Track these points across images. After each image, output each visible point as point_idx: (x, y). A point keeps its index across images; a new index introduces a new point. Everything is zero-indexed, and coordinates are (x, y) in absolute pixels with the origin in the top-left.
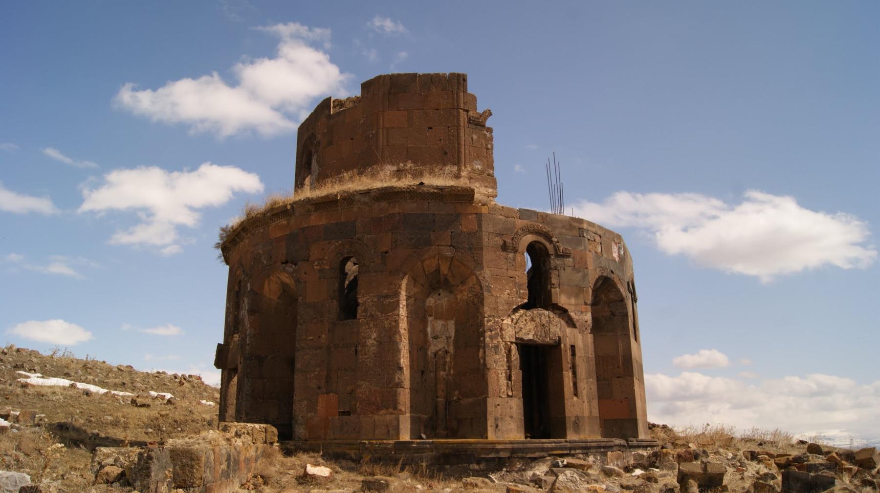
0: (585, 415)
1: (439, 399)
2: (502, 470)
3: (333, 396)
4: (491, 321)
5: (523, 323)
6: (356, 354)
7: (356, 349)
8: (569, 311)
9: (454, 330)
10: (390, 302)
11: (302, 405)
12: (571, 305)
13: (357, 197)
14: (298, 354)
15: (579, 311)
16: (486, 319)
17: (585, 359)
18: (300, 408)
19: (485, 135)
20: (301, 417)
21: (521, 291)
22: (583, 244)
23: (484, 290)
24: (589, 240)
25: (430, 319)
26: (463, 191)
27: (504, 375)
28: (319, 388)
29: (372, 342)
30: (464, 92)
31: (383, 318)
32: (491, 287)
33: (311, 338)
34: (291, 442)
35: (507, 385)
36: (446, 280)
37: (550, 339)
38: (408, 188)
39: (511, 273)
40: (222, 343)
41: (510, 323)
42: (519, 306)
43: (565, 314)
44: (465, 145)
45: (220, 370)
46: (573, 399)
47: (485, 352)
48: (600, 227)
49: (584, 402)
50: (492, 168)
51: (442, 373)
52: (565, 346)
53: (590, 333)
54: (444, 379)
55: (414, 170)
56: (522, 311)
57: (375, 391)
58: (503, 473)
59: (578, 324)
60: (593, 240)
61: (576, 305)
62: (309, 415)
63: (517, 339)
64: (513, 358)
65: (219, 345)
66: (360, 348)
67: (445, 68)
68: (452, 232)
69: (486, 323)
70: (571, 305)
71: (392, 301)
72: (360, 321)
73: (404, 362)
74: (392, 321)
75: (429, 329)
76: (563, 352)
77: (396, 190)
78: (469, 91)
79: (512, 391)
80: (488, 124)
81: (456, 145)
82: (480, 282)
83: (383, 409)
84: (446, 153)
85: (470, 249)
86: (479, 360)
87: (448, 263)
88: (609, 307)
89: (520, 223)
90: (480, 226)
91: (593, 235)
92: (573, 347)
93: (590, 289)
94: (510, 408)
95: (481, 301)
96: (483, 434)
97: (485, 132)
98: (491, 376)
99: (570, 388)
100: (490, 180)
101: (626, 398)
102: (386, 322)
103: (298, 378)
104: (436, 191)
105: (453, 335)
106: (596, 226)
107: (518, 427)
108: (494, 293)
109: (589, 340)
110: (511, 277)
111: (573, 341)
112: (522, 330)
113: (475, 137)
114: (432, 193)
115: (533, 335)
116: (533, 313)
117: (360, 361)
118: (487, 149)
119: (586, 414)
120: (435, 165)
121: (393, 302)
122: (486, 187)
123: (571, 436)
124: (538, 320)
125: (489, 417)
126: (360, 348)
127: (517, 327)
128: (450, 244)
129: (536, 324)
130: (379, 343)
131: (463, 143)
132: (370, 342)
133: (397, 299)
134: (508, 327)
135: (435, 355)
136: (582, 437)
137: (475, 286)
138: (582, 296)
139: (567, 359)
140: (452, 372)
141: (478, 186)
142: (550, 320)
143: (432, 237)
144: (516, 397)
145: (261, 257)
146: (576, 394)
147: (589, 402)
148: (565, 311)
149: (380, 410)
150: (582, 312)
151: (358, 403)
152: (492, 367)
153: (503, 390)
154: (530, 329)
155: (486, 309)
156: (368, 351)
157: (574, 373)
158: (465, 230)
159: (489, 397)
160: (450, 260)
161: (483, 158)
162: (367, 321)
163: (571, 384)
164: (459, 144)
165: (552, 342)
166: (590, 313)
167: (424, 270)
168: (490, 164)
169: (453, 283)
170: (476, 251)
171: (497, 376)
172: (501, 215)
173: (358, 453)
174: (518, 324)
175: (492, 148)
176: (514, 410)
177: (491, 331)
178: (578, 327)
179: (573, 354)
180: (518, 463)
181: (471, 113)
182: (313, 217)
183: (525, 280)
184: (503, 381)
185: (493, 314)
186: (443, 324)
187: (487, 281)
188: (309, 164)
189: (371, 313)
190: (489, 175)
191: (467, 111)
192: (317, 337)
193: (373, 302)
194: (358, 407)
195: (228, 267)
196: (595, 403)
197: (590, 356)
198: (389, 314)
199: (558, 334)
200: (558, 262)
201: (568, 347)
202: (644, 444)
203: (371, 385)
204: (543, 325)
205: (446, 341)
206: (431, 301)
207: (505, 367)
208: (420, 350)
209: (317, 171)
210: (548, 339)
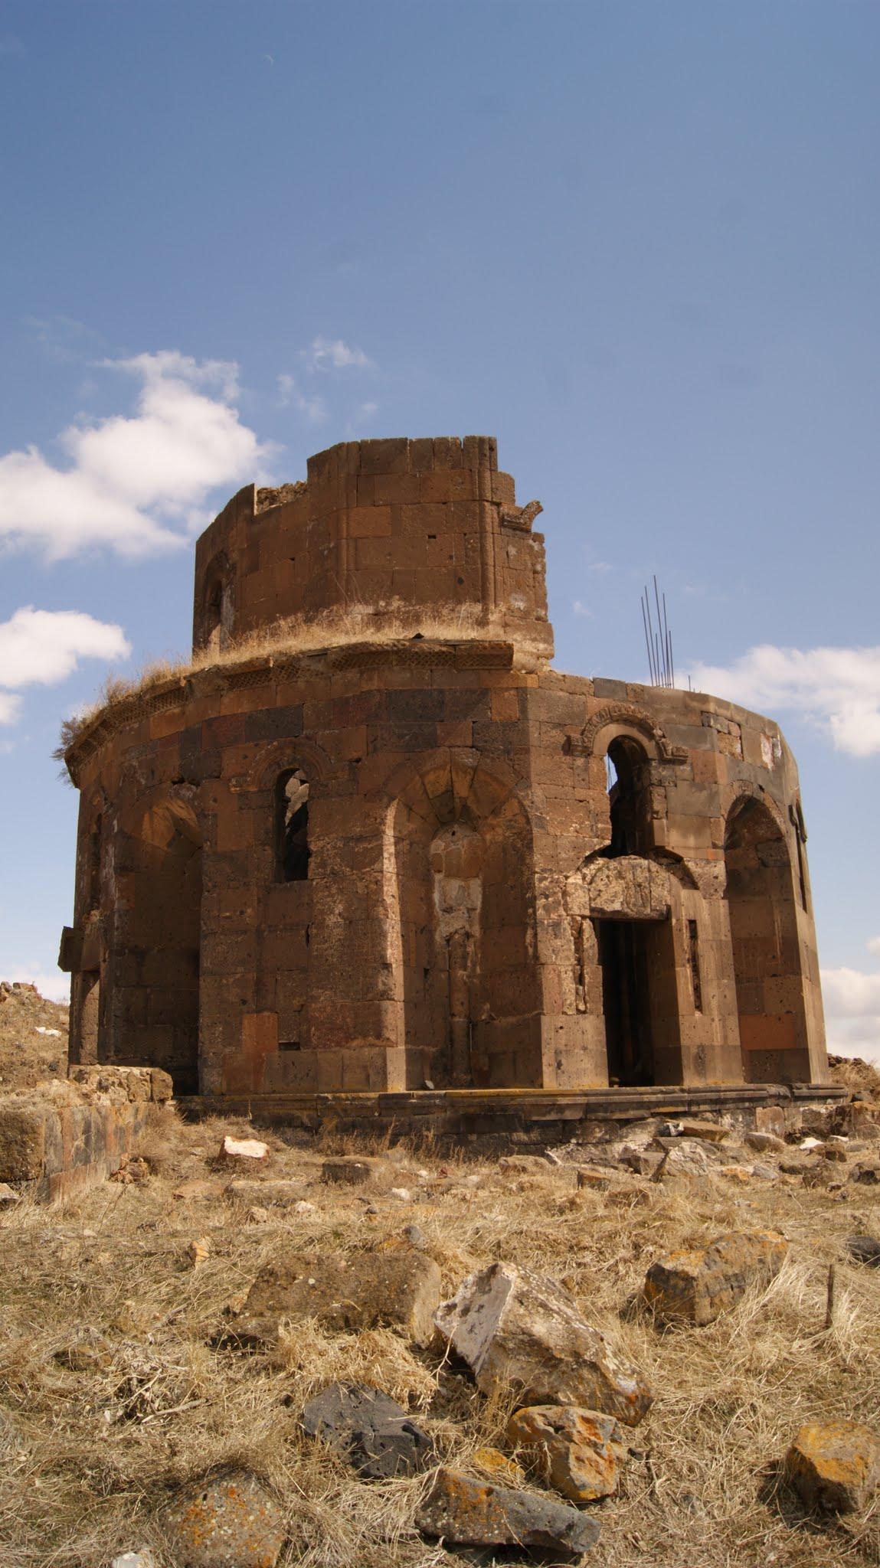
0: (715, 1044)
1: (456, 1019)
2: (570, 1142)
3: (269, 1017)
4: (545, 879)
5: (603, 883)
6: (308, 941)
7: (307, 931)
9: (480, 896)
10: (366, 849)
11: (214, 1034)
12: (689, 848)
13: (303, 663)
14: (206, 942)
15: (701, 859)
16: (537, 876)
17: (714, 947)
18: (211, 1039)
19: (532, 547)
20: (214, 1053)
21: (600, 825)
22: (708, 738)
23: (533, 824)
24: (719, 732)
25: (438, 877)
26: (493, 648)
27: (571, 974)
28: (244, 1002)
30: (491, 470)
31: (355, 877)
32: (545, 818)
33: (228, 914)
34: (196, 1098)
35: (577, 993)
36: (465, 808)
37: (651, 910)
38: (395, 646)
39: (581, 793)
40: (72, 926)
41: (580, 882)
42: (595, 851)
44: (494, 566)
45: (69, 974)
46: (694, 1015)
47: (536, 935)
48: (739, 709)
49: (713, 1020)
50: (545, 606)
51: (461, 972)
52: (679, 922)
53: (723, 898)
54: (465, 983)
55: (405, 613)
56: (601, 861)
57: (342, 1006)
58: (572, 1146)
59: (701, 882)
60: (726, 732)
61: (697, 848)
62: (227, 1050)
63: (592, 910)
64: (586, 945)
65: (66, 930)
66: (315, 931)
67: (457, 428)
68: (474, 722)
69: (537, 883)
70: (689, 848)
71: (369, 846)
72: (314, 883)
73: (393, 954)
75: (436, 896)
76: (675, 932)
77: (374, 649)
78: (500, 469)
79: (585, 1003)
80: (535, 528)
81: (479, 566)
82: (526, 811)
84: (461, 581)
85: (508, 752)
86: (526, 948)
87: (469, 778)
88: (757, 850)
89: (595, 704)
90: (524, 710)
91: (727, 722)
92: (692, 923)
93: (722, 819)
94: (583, 1033)
95: (529, 846)
96: (536, 1079)
97: (531, 542)
98: (548, 977)
99: (688, 995)
100: (542, 628)
101: (788, 1012)
102: (359, 884)
103: (206, 986)
104: (444, 649)
105: (479, 904)
106: (732, 707)
107: (596, 1065)
108: (551, 831)
109: (722, 910)
110: (581, 801)
111: (691, 912)
113: (512, 551)
114: (437, 653)
115: (622, 904)
116: (620, 863)
117: (315, 953)
118: (535, 572)
119: (718, 1040)
120: (441, 602)
121: (372, 848)
122: (534, 640)
123: (692, 1081)
124: (629, 876)
125: (544, 1050)
126: (315, 931)
127: (592, 889)
128: (470, 743)
129: (627, 883)
131: (491, 562)
132: (332, 920)
134: (576, 890)
135: (448, 941)
136: (711, 1081)
137: (517, 818)
138: (708, 832)
139: (682, 945)
140: (478, 970)
141: (519, 639)
142: (650, 876)
143: (439, 732)
144: (592, 1013)
145: (135, 772)
146: (699, 1007)
147: (723, 1020)
148: (678, 860)
149: (352, 1039)
150: (708, 862)
152: (549, 962)
153: (568, 1002)
155: (537, 857)
157: (696, 970)
158: (497, 718)
159: (544, 1014)
160: (472, 773)
161: (527, 589)
163: (691, 989)
164: (484, 564)
165: (654, 915)
166: (723, 863)
167: (425, 791)
168: (540, 600)
169: (478, 813)
170: (518, 756)
171: (559, 976)
172: (561, 690)
173: (315, 1116)
174: (594, 885)
175: (544, 570)
176: (590, 1036)
177: (547, 897)
178: (701, 887)
179: (694, 936)
180: (597, 1130)
181: (505, 509)
182: (226, 700)
183: (606, 806)
184: (569, 985)
185: (549, 867)
186: (460, 887)
187: (537, 809)
188: (217, 604)
189: (333, 868)
190: (538, 619)
191: (498, 505)
192: (238, 913)
193: (335, 848)
195: (78, 792)
196: (733, 1022)
197: (723, 938)
198: (365, 870)
200: (664, 773)
201: (685, 923)
202: (821, 1092)
204: (640, 885)
205: (466, 915)
206: (438, 846)
207: (573, 960)
208: (422, 933)
209: (233, 618)
210: (649, 910)
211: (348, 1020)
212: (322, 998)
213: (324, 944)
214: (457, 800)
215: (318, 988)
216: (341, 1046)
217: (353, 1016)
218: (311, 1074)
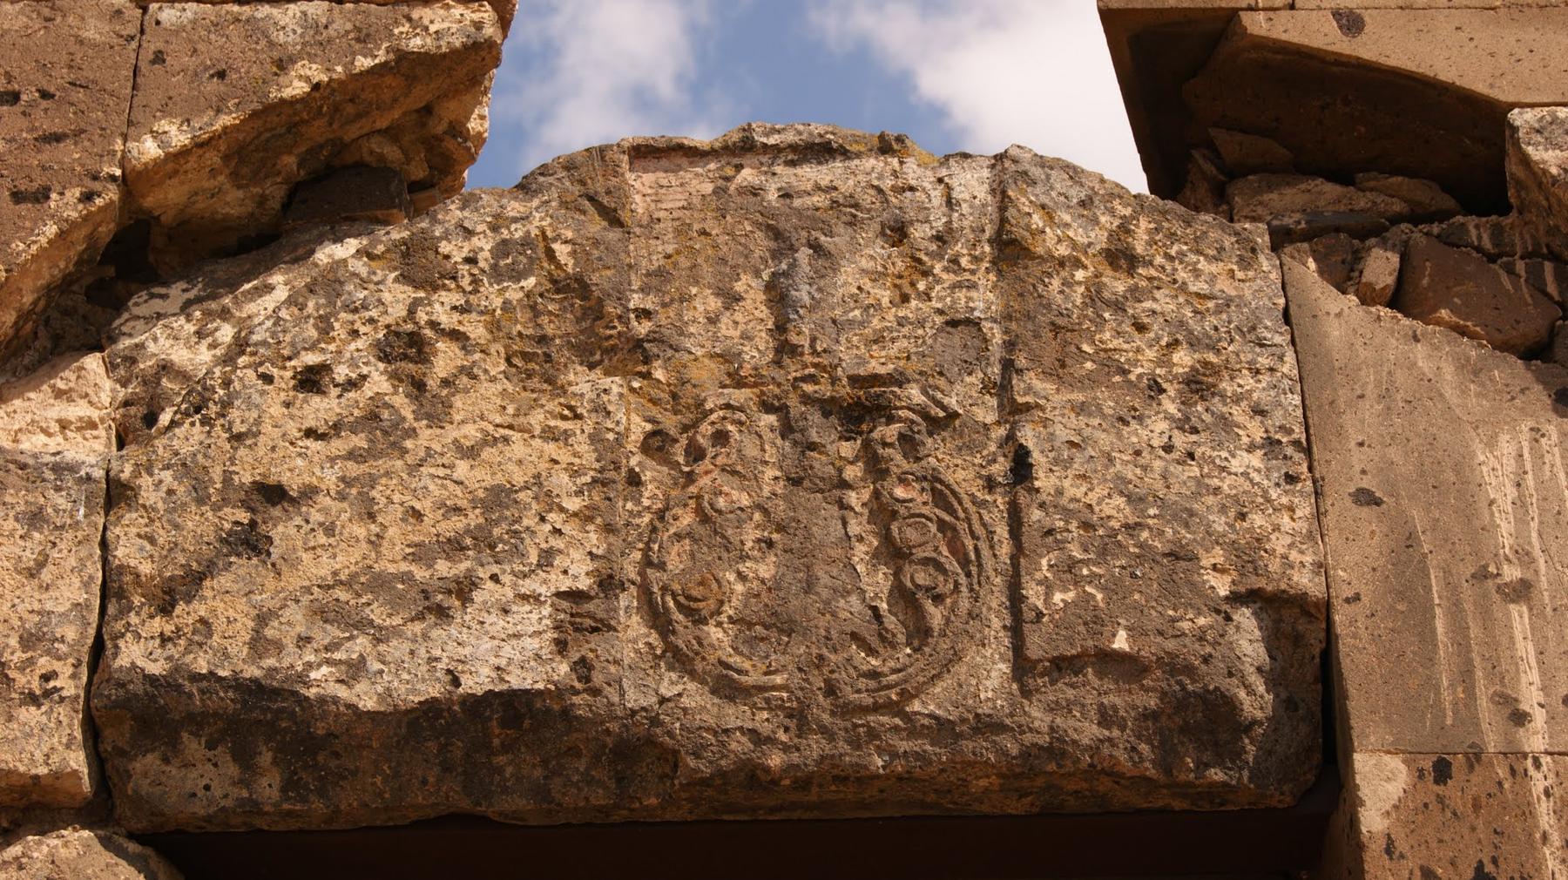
5: (321, 408)
8: (1521, 119)
37: (1022, 667)
43: (1477, 229)
112: (284, 531)
154: (498, 498)
199: (1247, 555)
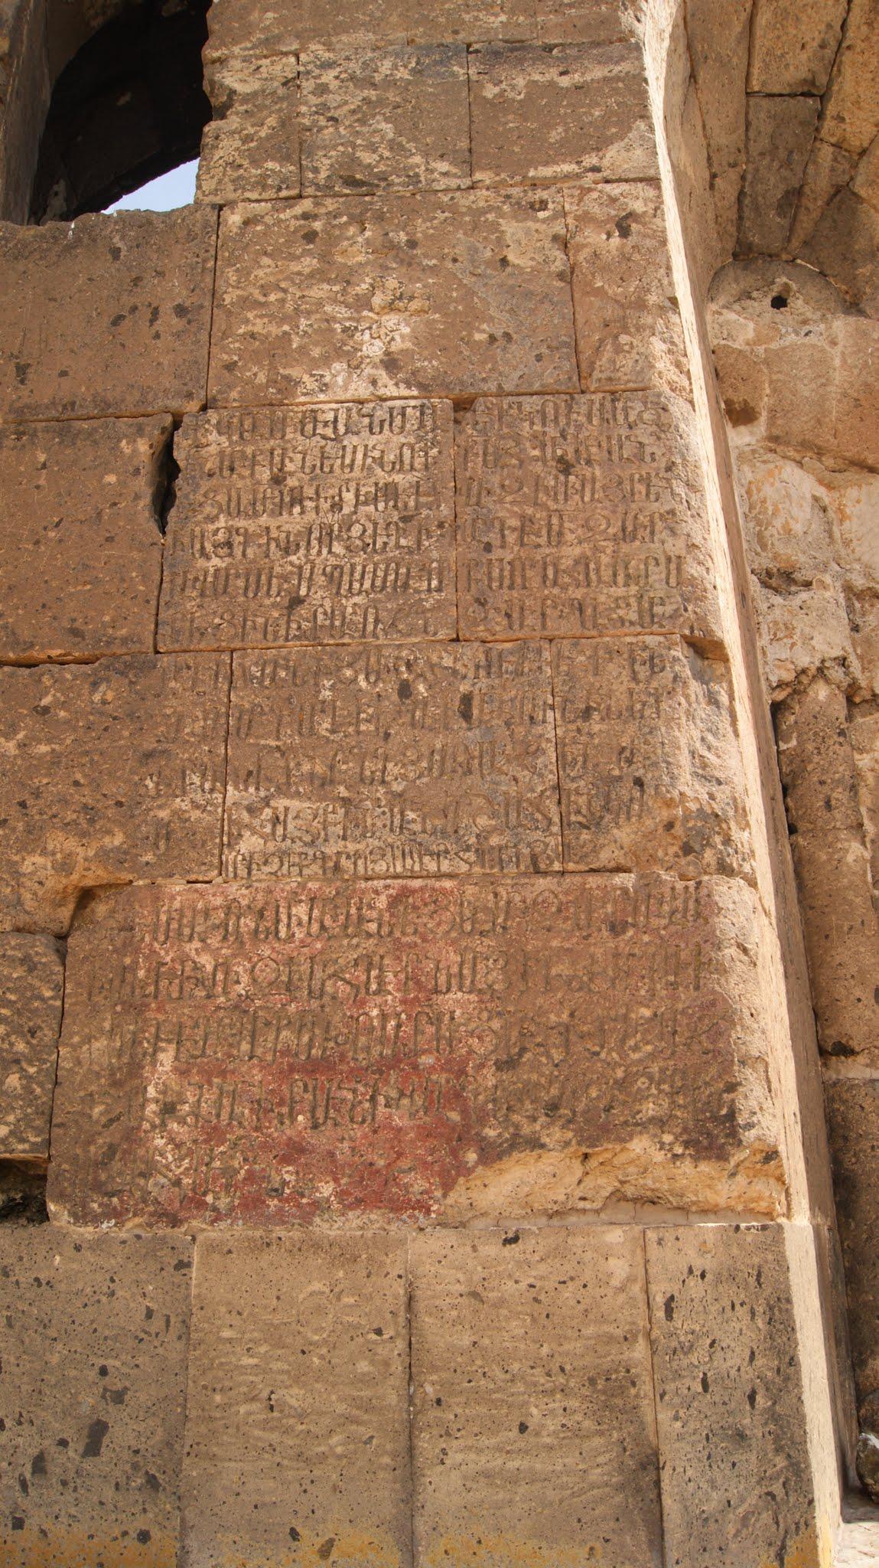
6: (164, 501)
29: (360, 388)
57: (394, 902)
66: (215, 442)
71: (565, 82)
72: (234, 219)
74: (585, 218)
83: (535, 1144)
102: (511, 228)
126: (215, 442)
130: (442, 404)
133: (625, 67)
149: (491, 1154)
151: (167, 1058)
156: (321, 469)
162: (306, 216)
194: (169, 1109)
203: (355, 825)
211: (455, 1002)
212: (249, 843)
213: (280, 509)
214: (826, 152)
215: (223, 774)
216: (398, 1206)
217: (492, 974)
218: (123, 1434)
